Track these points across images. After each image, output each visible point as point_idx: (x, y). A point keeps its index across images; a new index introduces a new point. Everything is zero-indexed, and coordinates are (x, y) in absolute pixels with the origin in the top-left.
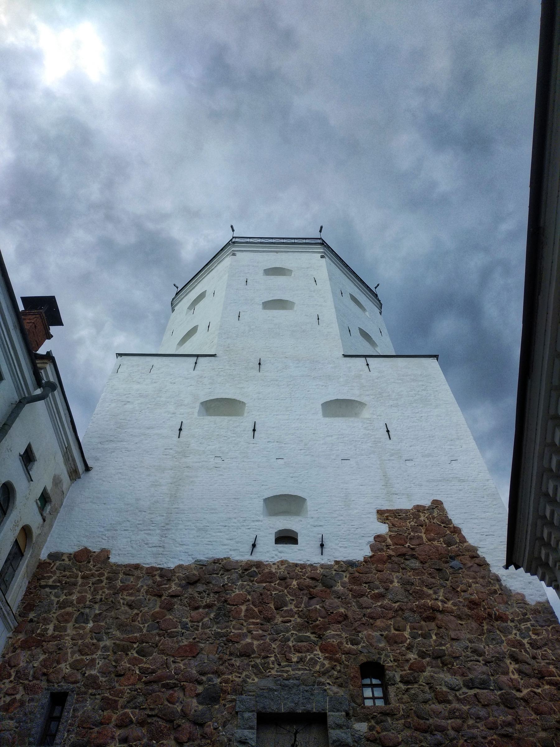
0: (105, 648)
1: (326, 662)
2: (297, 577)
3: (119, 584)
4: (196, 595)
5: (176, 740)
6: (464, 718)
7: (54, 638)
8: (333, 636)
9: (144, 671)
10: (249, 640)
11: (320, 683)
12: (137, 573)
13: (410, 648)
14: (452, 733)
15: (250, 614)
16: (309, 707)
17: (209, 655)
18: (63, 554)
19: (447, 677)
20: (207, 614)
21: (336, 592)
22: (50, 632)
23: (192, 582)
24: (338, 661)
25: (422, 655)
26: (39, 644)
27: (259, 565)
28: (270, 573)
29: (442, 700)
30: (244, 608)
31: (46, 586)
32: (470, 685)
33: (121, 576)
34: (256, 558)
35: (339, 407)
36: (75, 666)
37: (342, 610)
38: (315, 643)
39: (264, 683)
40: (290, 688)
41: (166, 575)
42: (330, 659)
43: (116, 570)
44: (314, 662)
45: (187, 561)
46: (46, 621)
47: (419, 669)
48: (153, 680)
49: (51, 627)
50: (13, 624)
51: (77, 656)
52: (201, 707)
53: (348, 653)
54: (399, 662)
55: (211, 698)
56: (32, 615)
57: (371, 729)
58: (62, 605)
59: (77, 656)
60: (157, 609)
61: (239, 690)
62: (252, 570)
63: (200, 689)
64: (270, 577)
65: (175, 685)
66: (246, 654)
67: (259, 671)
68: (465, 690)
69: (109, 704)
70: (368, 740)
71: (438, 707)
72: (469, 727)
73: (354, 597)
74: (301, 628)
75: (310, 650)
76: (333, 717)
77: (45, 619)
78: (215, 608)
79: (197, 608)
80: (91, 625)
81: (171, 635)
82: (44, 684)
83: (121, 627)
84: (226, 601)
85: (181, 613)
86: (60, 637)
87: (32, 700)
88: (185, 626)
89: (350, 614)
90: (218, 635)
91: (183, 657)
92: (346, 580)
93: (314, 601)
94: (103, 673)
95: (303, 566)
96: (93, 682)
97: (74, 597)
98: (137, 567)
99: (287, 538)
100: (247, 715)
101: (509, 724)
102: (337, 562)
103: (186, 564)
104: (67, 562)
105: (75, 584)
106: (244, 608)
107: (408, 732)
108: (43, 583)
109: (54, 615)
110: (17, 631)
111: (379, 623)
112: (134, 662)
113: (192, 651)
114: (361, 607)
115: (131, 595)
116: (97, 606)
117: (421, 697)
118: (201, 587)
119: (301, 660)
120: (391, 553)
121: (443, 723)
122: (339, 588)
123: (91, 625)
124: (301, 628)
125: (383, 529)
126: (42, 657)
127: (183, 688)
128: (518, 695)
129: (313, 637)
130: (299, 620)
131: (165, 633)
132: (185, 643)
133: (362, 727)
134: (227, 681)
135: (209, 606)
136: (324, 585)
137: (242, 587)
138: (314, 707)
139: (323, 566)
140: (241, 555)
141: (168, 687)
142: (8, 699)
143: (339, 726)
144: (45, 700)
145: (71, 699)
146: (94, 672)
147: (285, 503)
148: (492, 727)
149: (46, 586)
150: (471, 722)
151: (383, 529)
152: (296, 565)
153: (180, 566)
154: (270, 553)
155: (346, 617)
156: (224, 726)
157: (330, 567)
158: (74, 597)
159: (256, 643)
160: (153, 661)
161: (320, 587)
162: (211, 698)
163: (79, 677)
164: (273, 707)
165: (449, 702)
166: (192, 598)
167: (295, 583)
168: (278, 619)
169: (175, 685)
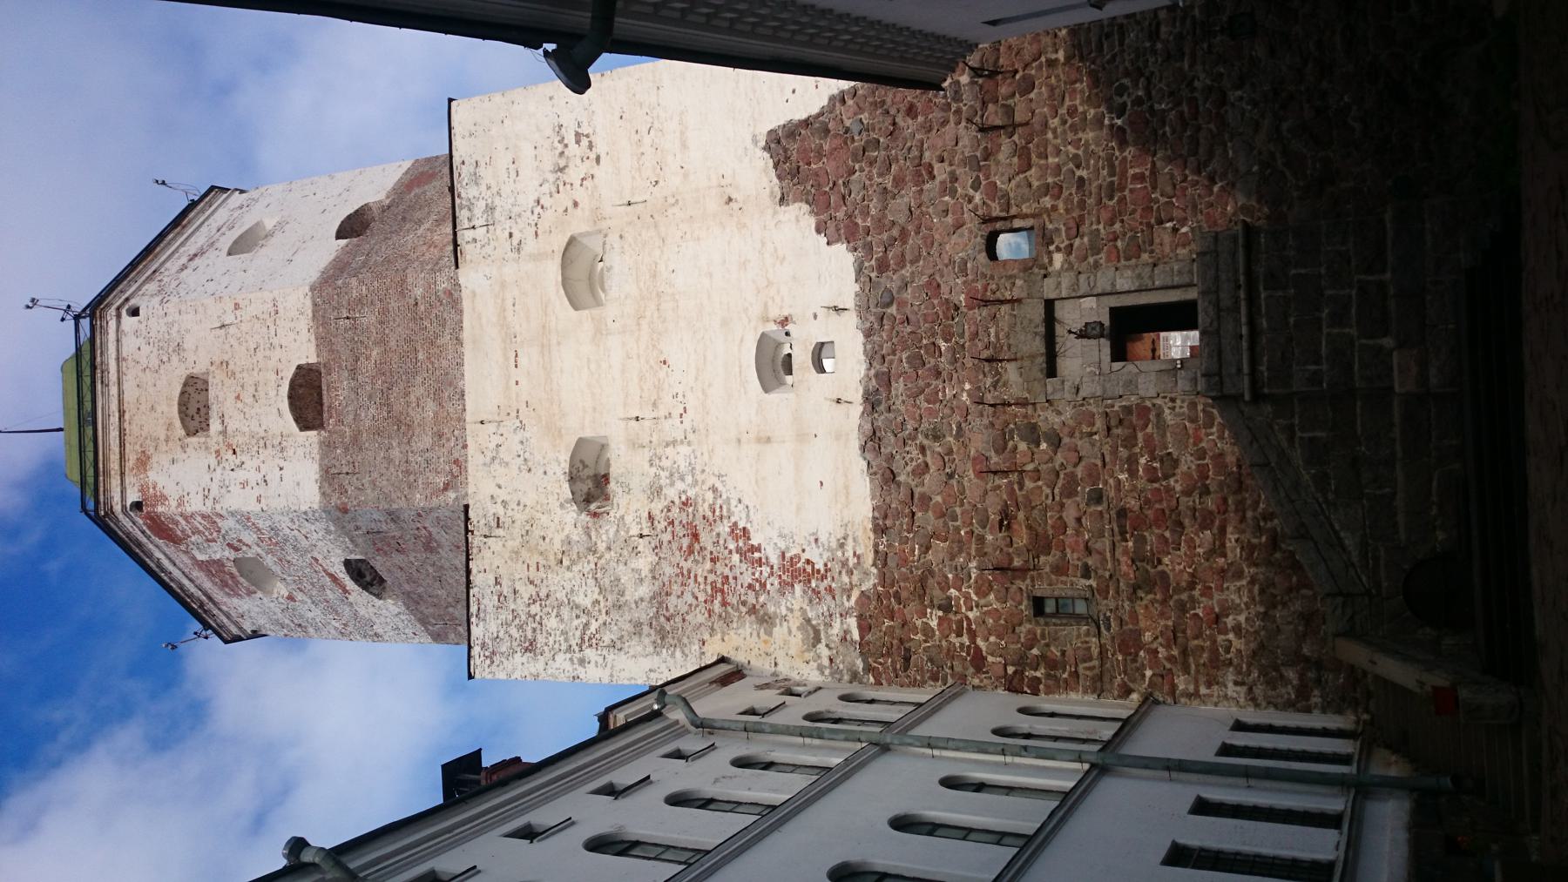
4: (909, 468)
5: (1076, 465)
34: (857, 395)
57: (1058, 249)
62: (872, 402)
63: (1023, 446)
70: (1070, 253)
72: (1056, 137)
78: (926, 442)
79: (927, 465)
120: (840, 215)
133: (1058, 259)
135: (923, 449)
136: (889, 304)
138: (1038, 313)
147: (775, 366)
161: (893, 310)
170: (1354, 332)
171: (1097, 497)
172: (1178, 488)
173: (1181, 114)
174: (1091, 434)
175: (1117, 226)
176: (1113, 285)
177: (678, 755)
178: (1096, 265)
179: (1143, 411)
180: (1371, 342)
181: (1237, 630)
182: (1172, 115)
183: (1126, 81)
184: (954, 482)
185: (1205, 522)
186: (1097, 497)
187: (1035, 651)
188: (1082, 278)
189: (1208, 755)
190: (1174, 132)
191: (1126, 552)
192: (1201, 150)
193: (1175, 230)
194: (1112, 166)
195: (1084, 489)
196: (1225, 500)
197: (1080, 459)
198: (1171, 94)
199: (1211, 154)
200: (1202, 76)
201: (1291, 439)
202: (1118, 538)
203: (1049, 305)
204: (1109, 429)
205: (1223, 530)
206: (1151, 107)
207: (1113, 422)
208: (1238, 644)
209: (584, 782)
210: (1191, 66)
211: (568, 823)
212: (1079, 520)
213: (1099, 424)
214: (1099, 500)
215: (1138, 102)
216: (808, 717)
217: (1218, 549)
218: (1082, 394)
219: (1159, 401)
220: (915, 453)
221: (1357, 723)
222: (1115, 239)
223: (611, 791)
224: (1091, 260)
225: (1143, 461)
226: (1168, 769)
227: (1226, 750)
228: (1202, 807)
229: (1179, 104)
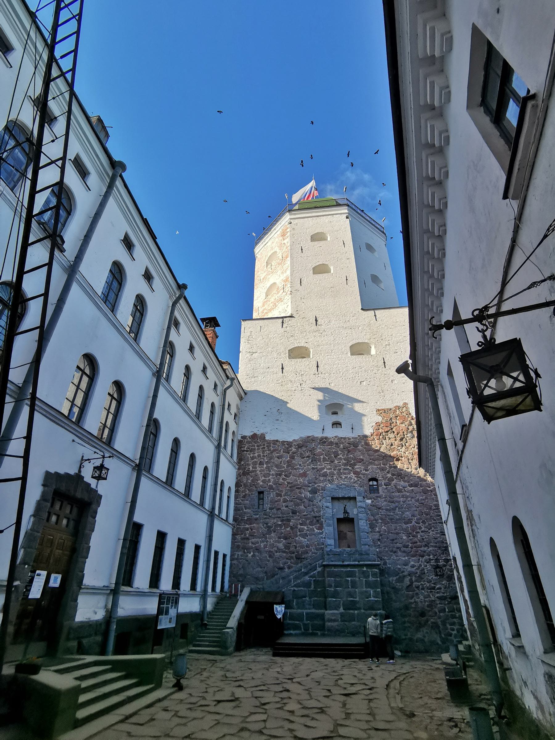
0: (273, 475)
1: (356, 478)
2: (343, 443)
3: (272, 449)
6: (407, 497)
7: (253, 471)
8: (358, 468)
9: (288, 483)
10: (325, 470)
11: (353, 486)
12: (278, 443)
13: (388, 472)
14: (402, 503)
15: (324, 460)
16: (349, 495)
17: (311, 475)
18: (246, 436)
19: (402, 483)
20: (308, 460)
21: (359, 449)
22: (251, 469)
23: (300, 446)
24: (360, 478)
25: (393, 475)
26: (248, 474)
27: (326, 438)
28: (331, 441)
29: (399, 491)
30: (322, 457)
31: (244, 451)
32: (411, 486)
33: (272, 445)
34: (325, 435)
35: (359, 349)
36: (263, 481)
37: (362, 457)
38: (351, 471)
39: (332, 487)
40: (342, 489)
41: (290, 444)
42: (357, 477)
43: (269, 442)
44: (351, 478)
45: (297, 438)
46: (249, 465)
47: (391, 480)
48: (293, 487)
49: (251, 467)
50: (237, 467)
51: (263, 478)
52: (311, 495)
53: (364, 474)
54: (384, 478)
55: (314, 491)
56: (242, 463)
57: (372, 502)
58: (253, 458)
59: (263, 478)
60: (289, 459)
61: (324, 489)
62: (324, 441)
64: (331, 443)
65: (301, 488)
66: (325, 475)
67: (331, 482)
68: (409, 488)
69: (279, 495)
71: (398, 494)
73: (366, 451)
74: (345, 465)
75: (349, 474)
76: (359, 498)
77: (248, 464)
80: (265, 466)
81: (295, 469)
82: (254, 488)
83: (277, 466)
84: (314, 454)
85: (298, 460)
86: (256, 471)
87: (252, 494)
88: (300, 465)
89: (364, 459)
90: (313, 469)
91: (302, 477)
92: (363, 443)
93: (349, 453)
94: (274, 484)
95: (345, 438)
96: (271, 487)
97: (256, 455)
98: (277, 441)
99: (337, 424)
100: (328, 498)
101: (423, 500)
102: (359, 436)
103: (296, 439)
104: (249, 439)
105: (255, 449)
106: (322, 457)
107: (385, 503)
108: (242, 449)
109: (250, 462)
110: (239, 469)
111: (376, 462)
112: (283, 479)
113: (304, 475)
114: (369, 455)
115: (277, 453)
116: (265, 458)
117: (392, 491)
118: (304, 449)
119: (346, 477)
121: (399, 500)
122: (360, 447)
123: (265, 466)
124: (345, 465)
125: (379, 419)
126: (251, 479)
127: (304, 489)
128: (429, 489)
129: (350, 468)
130: (344, 461)
131: (293, 468)
132: (302, 472)
133: (369, 501)
134: (319, 486)
137: (320, 448)
138: (352, 495)
139: (353, 438)
140: (318, 434)
141: (298, 488)
142: (244, 494)
143: (361, 502)
144: (257, 494)
145: (265, 493)
146: (271, 484)
148: (418, 500)
149: (244, 451)
150: (409, 499)
151: (379, 419)
152: (342, 438)
153: (294, 440)
154: (331, 433)
155: (363, 460)
156: (320, 501)
157: (356, 438)
158: (256, 455)
159: (328, 471)
160: (291, 479)
161: (352, 447)
162: (314, 491)
163: (266, 486)
164: (337, 495)
165: (402, 492)
166: (301, 454)
167: (342, 446)
168: (336, 462)
169: (301, 488)
170: (345, 599)
171: (294, 512)
172: (297, 538)
173: (417, 543)
174: (313, 511)
175: (380, 521)
176: (361, 519)
177: (216, 385)
178: (367, 514)
179: (321, 528)
180: (341, 604)
181: (253, 556)
182: (416, 539)
183: (427, 524)
184: (298, 466)
185: (287, 547)
186: (294, 512)
187: (248, 491)
188: (363, 510)
189: (215, 547)
190: (410, 540)
191: (277, 521)
192: (405, 549)
193: (379, 540)
194: (399, 519)
195: (297, 508)
196: (294, 553)
197: (306, 507)
198: (423, 539)
199: (404, 552)
200: (429, 550)
201: (311, 577)
202: (282, 519)
203: (354, 498)
204: (315, 517)
205: (284, 552)
206: (419, 532)
207: (317, 518)
208: (250, 555)
209: (207, 360)
210: (432, 546)
211: (194, 359)
212: (287, 507)
213: (317, 514)
214: (293, 513)
215: (420, 528)
216: (227, 423)
217: (279, 550)
218: (326, 509)
219: (324, 534)
220: (307, 454)
221: (226, 592)
222: (376, 520)
223: (204, 369)
224: (369, 512)
225: (306, 528)
226: (210, 536)
227: (216, 553)
228: (197, 548)
229: (420, 541)
